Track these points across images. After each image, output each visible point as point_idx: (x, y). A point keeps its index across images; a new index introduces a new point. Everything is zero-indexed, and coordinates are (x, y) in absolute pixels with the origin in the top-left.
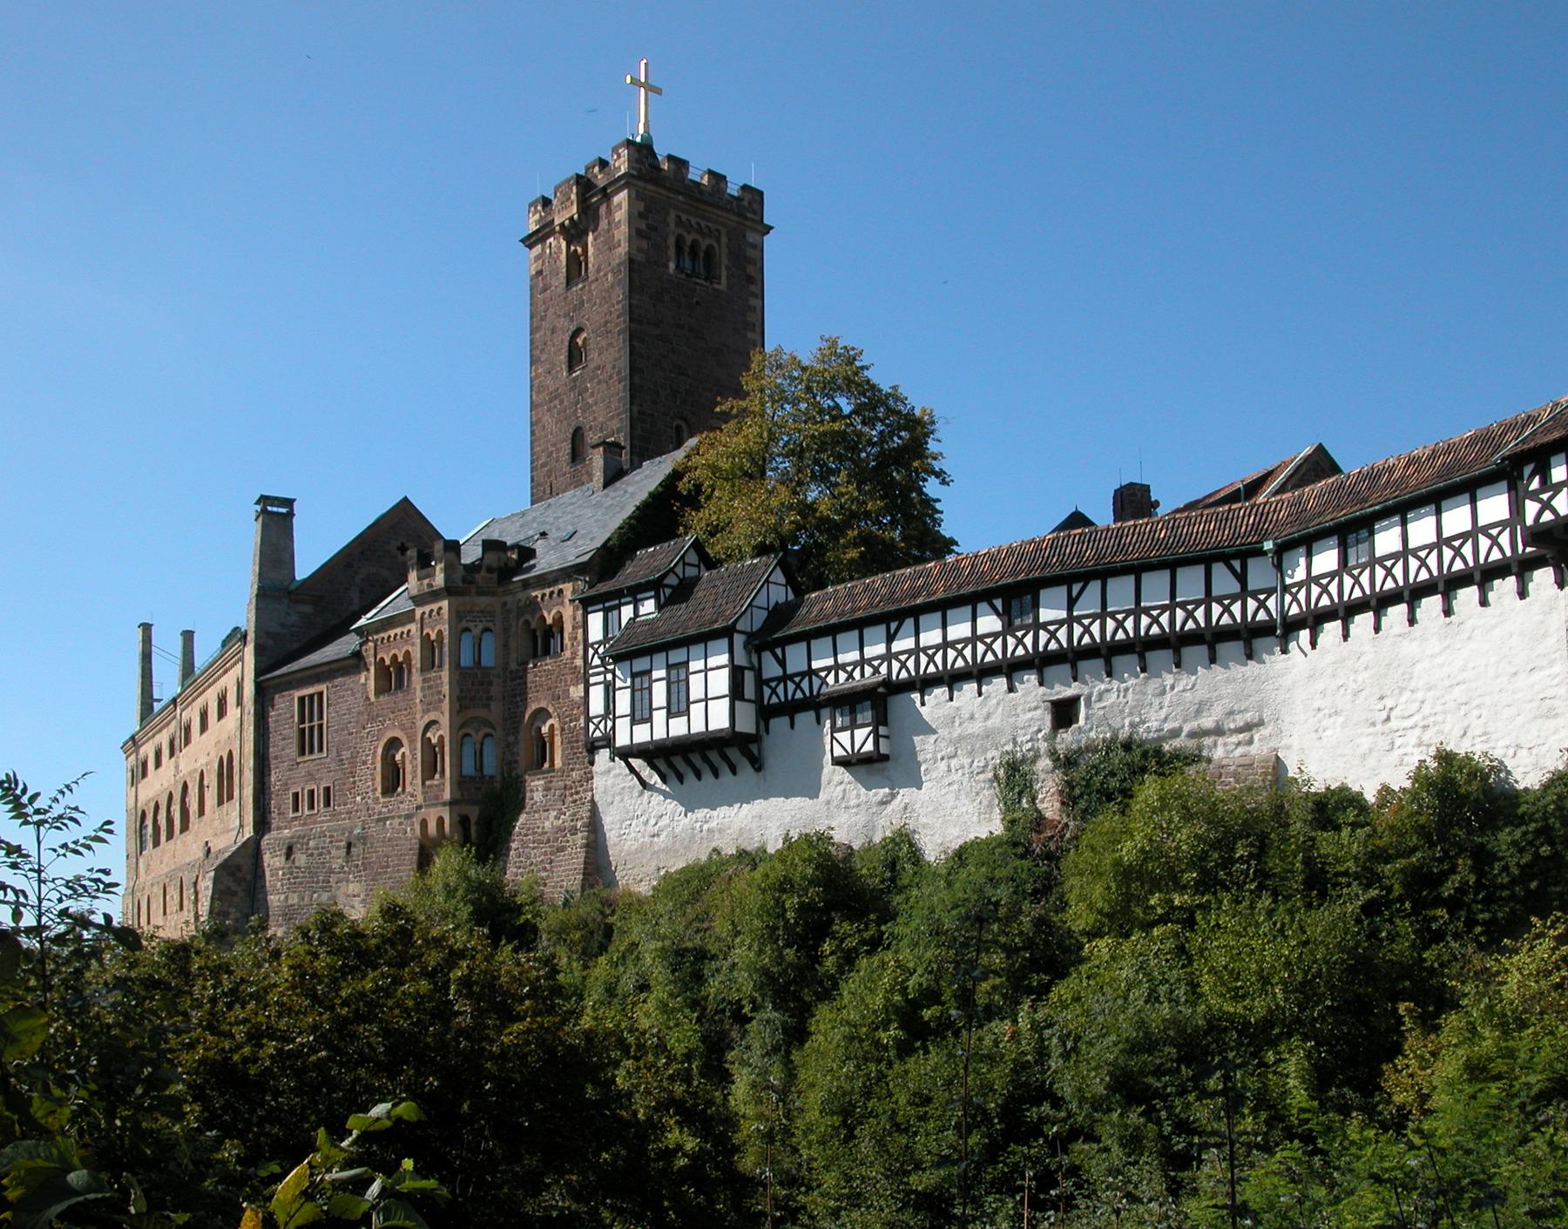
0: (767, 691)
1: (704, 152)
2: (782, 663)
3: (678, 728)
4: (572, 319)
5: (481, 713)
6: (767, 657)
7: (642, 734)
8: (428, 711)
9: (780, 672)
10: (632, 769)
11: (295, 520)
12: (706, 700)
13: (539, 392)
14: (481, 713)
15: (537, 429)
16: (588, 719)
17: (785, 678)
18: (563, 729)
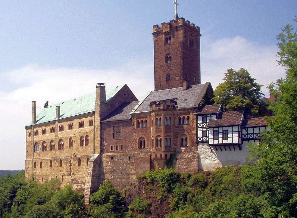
0: (243, 136)
1: (194, 21)
2: (247, 131)
3: (225, 142)
4: (166, 52)
5: (169, 134)
6: (244, 130)
7: (216, 142)
8: (157, 133)
9: (247, 133)
10: (211, 148)
11: (106, 88)
12: (232, 137)
13: (157, 65)
14: (169, 134)
15: (156, 72)
16: (197, 137)
17: (248, 134)
18: (190, 139)
